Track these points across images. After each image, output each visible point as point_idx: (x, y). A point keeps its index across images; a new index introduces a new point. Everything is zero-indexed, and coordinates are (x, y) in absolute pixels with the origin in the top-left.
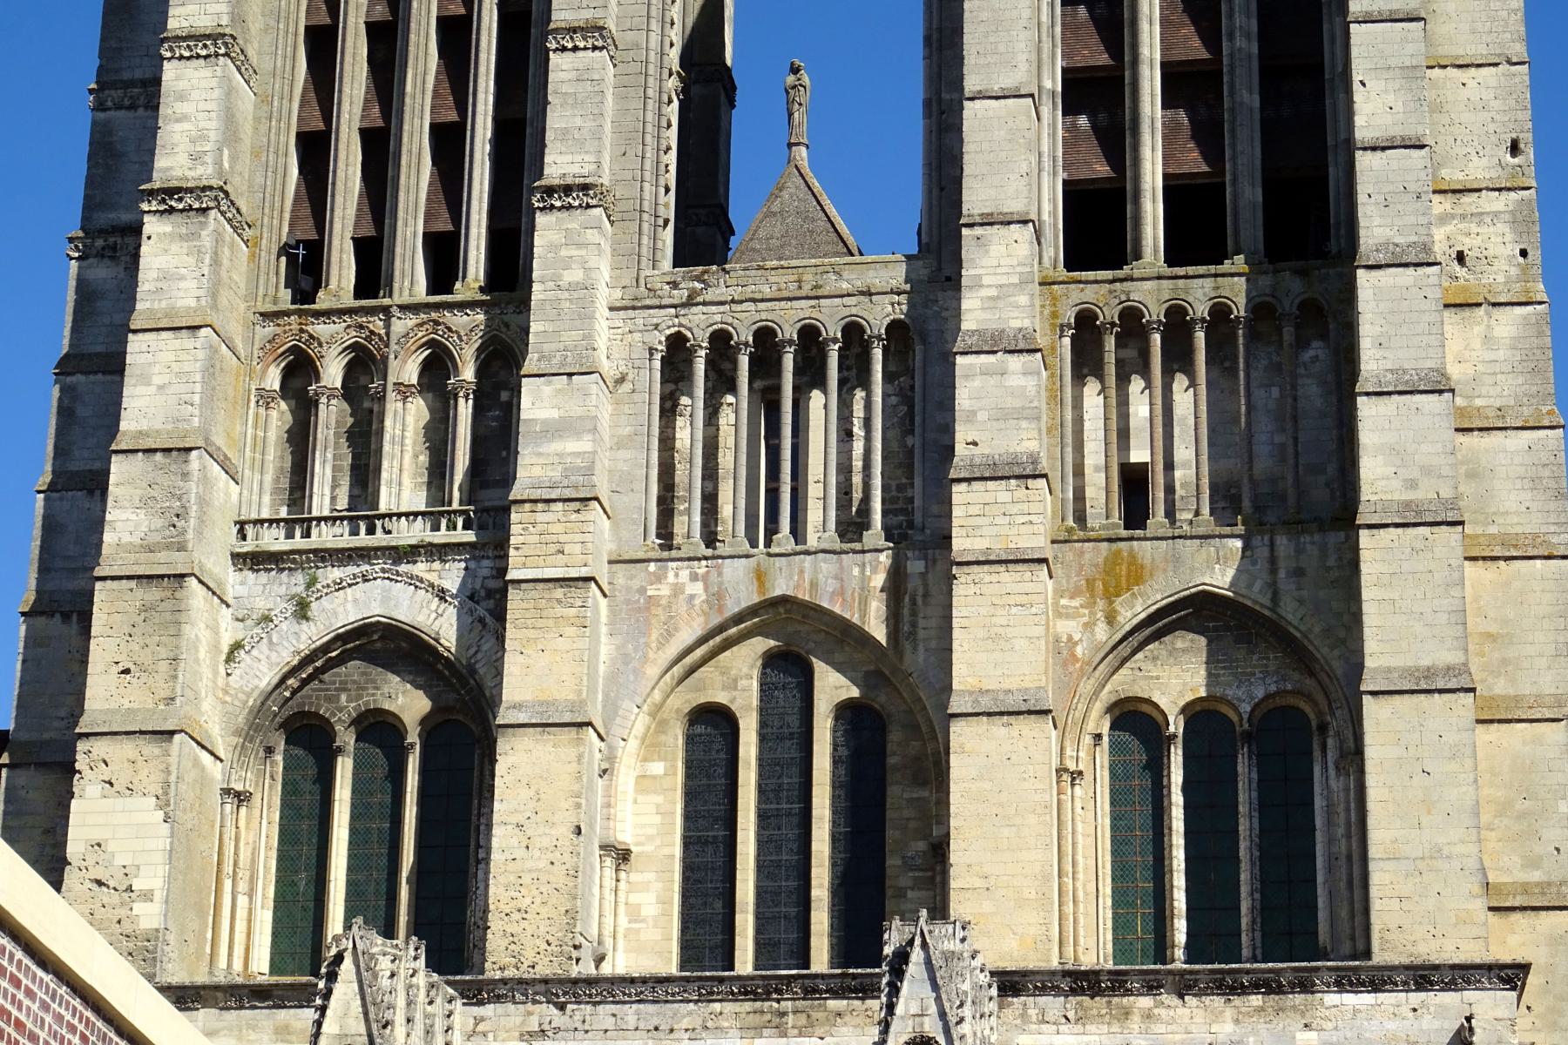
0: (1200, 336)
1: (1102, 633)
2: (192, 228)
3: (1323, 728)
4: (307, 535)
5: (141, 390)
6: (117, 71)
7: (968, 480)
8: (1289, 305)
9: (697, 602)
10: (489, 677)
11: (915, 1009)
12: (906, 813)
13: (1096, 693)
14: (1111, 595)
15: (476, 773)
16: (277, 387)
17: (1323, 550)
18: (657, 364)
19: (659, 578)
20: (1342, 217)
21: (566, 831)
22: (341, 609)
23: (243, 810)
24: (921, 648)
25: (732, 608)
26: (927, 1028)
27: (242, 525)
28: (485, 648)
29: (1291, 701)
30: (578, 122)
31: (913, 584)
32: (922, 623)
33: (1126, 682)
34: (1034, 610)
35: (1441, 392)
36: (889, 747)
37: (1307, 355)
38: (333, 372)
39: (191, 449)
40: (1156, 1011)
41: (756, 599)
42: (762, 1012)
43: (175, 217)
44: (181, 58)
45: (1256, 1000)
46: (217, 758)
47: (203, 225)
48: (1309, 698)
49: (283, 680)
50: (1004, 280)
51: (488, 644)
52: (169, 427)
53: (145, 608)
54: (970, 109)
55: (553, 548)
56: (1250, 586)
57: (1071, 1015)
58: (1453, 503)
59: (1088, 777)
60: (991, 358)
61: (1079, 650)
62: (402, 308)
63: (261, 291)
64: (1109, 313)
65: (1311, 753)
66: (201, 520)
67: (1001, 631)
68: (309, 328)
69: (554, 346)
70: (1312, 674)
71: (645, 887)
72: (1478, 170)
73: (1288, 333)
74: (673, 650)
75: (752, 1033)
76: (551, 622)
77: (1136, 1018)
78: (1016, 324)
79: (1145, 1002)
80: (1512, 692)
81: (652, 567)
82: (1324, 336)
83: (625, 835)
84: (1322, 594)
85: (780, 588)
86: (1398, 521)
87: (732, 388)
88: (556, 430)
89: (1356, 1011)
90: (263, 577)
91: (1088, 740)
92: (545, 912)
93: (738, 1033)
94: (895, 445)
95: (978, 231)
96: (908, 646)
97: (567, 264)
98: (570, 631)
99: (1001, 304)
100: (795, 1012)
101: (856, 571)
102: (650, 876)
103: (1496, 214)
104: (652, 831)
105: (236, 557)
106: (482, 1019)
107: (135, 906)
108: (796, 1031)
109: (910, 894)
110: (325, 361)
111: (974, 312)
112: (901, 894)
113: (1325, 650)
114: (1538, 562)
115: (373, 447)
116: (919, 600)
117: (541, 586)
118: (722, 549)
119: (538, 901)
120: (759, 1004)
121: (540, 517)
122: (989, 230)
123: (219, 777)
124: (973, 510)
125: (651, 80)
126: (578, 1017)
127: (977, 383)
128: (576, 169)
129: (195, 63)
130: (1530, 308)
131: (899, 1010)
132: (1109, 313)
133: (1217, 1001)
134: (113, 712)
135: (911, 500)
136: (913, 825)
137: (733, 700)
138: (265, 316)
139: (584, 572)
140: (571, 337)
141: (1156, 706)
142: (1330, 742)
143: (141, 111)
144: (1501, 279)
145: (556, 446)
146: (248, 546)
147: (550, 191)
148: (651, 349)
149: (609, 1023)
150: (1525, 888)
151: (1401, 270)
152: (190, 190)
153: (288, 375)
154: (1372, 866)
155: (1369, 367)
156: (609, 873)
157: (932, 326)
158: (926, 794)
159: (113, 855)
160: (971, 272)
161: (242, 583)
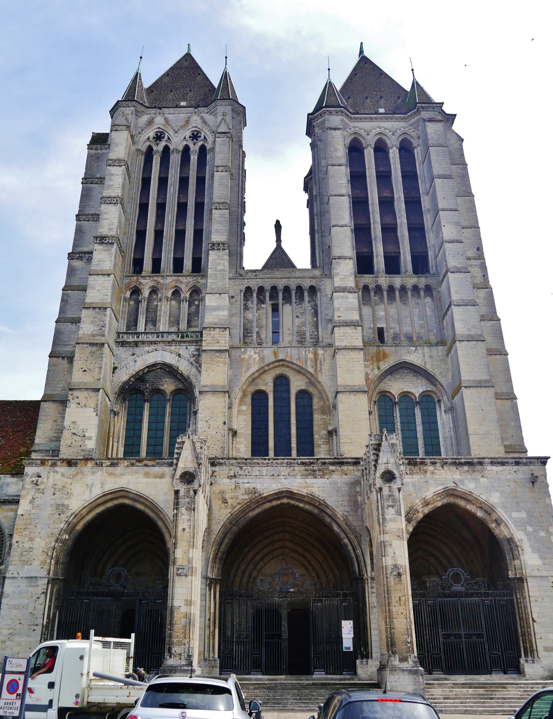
0: (397, 293)
1: (376, 372)
2: (109, 248)
3: (439, 401)
4: (138, 337)
5: (92, 291)
6: (84, 211)
8: (422, 286)
9: (256, 360)
10: (194, 379)
11: (385, 461)
12: (320, 423)
13: (375, 389)
14: (378, 360)
15: (188, 408)
16: (129, 296)
17: (438, 352)
18: (242, 294)
19: (245, 353)
20: (434, 264)
21: (221, 423)
22: (148, 359)
23: (116, 417)
24: (324, 375)
25: (267, 362)
26: (390, 467)
27: (118, 333)
28: (192, 371)
29: (429, 393)
30: (221, 228)
31: (320, 356)
32: (323, 368)
33: (383, 386)
35: (475, 306)
37: (426, 300)
38: (146, 293)
39: (107, 308)
41: (274, 360)
42: (308, 470)
43: (103, 245)
45: (466, 468)
46: (110, 400)
48: (435, 393)
49: (130, 378)
50: (345, 274)
51: (194, 370)
52: (101, 301)
53: (91, 352)
54: (333, 229)
55: (216, 341)
56: (418, 360)
57: (408, 472)
58: (481, 335)
59: (373, 413)
61: (370, 377)
62: (167, 276)
63: (125, 270)
64: (372, 286)
65: (435, 409)
66: (109, 329)
68: (140, 281)
69: (215, 286)
70: (435, 386)
71: (241, 443)
73: (422, 293)
75: (305, 477)
76: (215, 362)
77: (429, 473)
78: (350, 285)
79: (431, 468)
81: (243, 350)
82: (431, 296)
84: (439, 363)
85: (281, 357)
87: (263, 302)
88: (215, 309)
89: (497, 472)
90: (124, 349)
91: (373, 403)
92: (215, 447)
93: (300, 477)
94: (311, 320)
95: (337, 260)
96: (319, 374)
97: (219, 264)
98: (221, 365)
99: (345, 280)
100: (319, 470)
101: (304, 353)
102: (242, 439)
103: (475, 265)
104: (243, 426)
105: (116, 342)
106: (215, 471)
107: (86, 441)
108: (319, 477)
109: (322, 446)
110: (145, 290)
111: (338, 282)
112: (319, 446)
113: (441, 378)
115: (158, 314)
116: (322, 361)
117: (212, 352)
118: (263, 345)
119: (213, 444)
121: (212, 332)
122: (340, 260)
123: (110, 406)
124: (341, 335)
125: (239, 221)
126: (247, 471)
127: (340, 300)
128: (221, 240)
131: (380, 461)
132: (372, 286)
133: (453, 468)
134: (81, 382)
135: (318, 335)
136: (322, 426)
137: (267, 389)
139: (225, 348)
140: (220, 284)
141: (392, 394)
142: (442, 405)
143: (91, 222)
145: (216, 313)
146: (121, 340)
147: (213, 244)
149: (257, 473)
152: (109, 237)
153: (132, 294)
154: (470, 436)
156: (231, 438)
157: (322, 287)
158: (325, 417)
159: (79, 425)
160: (336, 271)
161: (119, 350)
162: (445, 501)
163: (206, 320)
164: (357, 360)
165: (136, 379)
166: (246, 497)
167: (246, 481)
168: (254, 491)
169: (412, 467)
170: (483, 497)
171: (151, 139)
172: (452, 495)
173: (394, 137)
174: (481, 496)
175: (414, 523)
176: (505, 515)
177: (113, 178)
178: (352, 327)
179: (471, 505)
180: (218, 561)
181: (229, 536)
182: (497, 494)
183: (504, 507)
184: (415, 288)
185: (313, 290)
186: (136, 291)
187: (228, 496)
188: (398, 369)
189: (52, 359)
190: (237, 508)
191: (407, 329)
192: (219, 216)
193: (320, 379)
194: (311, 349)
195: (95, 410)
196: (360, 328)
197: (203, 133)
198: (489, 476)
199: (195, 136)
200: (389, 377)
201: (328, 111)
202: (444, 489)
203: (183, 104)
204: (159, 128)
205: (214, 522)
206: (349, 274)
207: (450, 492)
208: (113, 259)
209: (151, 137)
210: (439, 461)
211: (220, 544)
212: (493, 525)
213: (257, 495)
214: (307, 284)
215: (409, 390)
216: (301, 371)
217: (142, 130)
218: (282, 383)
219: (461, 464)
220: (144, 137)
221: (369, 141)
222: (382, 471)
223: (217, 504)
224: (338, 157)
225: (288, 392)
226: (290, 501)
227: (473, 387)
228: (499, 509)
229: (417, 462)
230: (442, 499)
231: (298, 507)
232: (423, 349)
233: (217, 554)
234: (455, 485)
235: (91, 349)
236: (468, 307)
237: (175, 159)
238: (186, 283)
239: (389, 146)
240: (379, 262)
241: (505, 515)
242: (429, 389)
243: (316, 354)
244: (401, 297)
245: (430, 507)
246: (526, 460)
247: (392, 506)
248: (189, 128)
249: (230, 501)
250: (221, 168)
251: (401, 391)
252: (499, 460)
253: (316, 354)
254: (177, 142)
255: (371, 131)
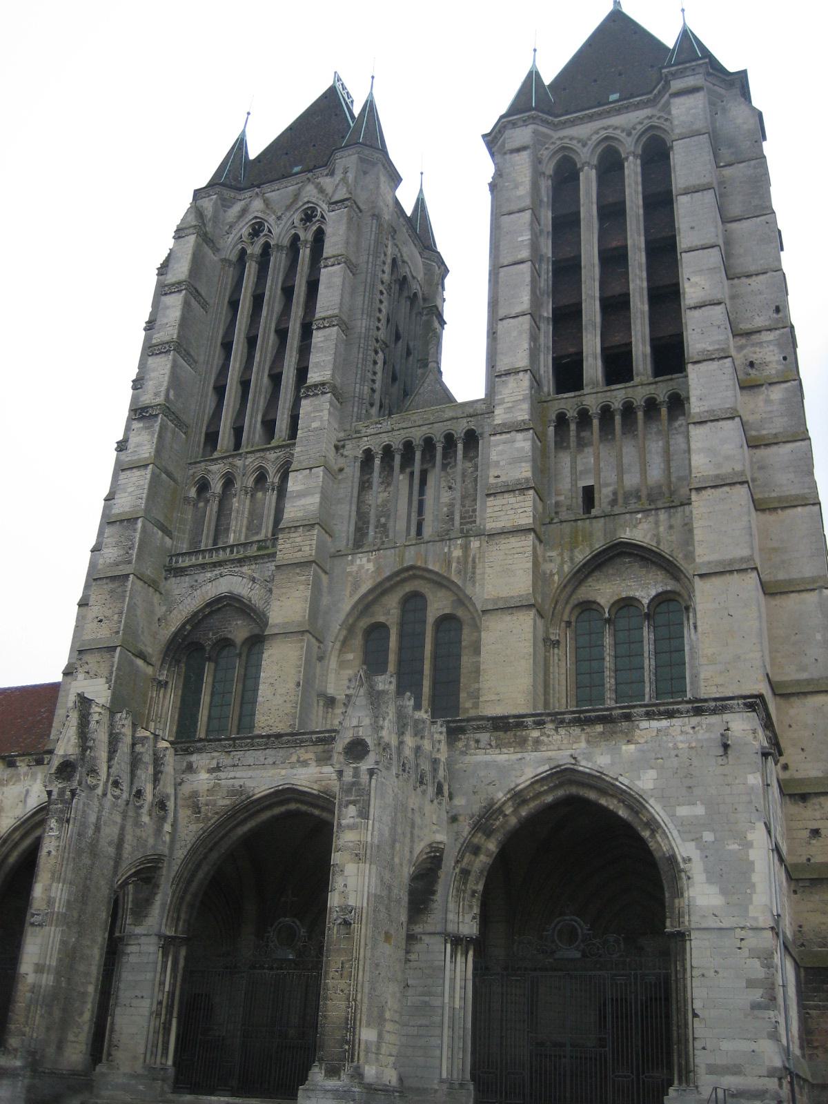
0: (618, 419)
5: (123, 495)
7: (494, 494)
11: (355, 723)
14: (573, 546)
18: (358, 464)
19: (352, 562)
21: (292, 685)
23: (162, 691)
33: (584, 593)
34: (526, 555)
35: (733, 418)
36: (464, 637)
37: (677, 424)
38: (217, 486)
39: (138, 518)
40: (542, 738)
41: (398, 567)
44: (157, 354)
45: (599, 728)
47: (156, 422)
49: (184, 625)
53: (112, 591)
57: (493, 743)
60: (508, 436)
62: (247, 453)
64: (571, 414)
65: (683, 624)
67: (509, 567)
72: (759, 322)
73: (664, 411)
74: (356, 598)
78: (520, 418)
79: (535, 734)
80: (787, 577)
81: (350, 558)
83: (331, 691)
86: (711, 484)
88: (301, 495)
89: (659, 731)
91: (563, 624)
95: (504, 378)
111: (500, 416)
114: (799, 509)
116: (477, 560)
120: (327, 746)
124: (497, 509)
126: (236, 759)
127: (500, 448)
129: (160, 356)
130: (789, 384)
132: (571, 414)
133: (576, 731)
138: (190, 464)
139: (311, 559)
141: (599, 604)
144: (773, 372)
145: (303, 501)
147: (309, 388)
148: (355, 457)
149: (251, 761)
150: (798, 682)
151: (710, 362)
152: (152, 407)
155: (695, 411)
160: (500, 397)
162: (560, 793)
163: (286, 516)
164: (519, 550)
165: (192, 627)
166: (227, 802)
167: (232, 775)
168: (240, 791)
169: (501, 734)
170: (624, 781)
171: (244, 239)
172: (571, 782)
173: (629, 139)
174: (621, 779)
175: (499, 836)
176: (662, 813)
177: (167, 312)
178: (517, 492)
179: (609, 798)
180: (184, 908)
181: (205, 867)
182: (652, 774)
183: (663, 798)
184: (651, 406)
185: (472, 439)
186: (203, 486)
187: (202, 800)
188: (611, 558)
189: (82, 608)
190: (212, 821)
191: (632, 480)
192: (323, 339)
193: (469, 591)
194: (459, 542)
195: (108, 681)
196: (531, 492)
197: (319, 210)
198: (642, 741)
199: (309, 216)
200: (596, 574)
201: (509, 122)
202: (551, 769)
203: (296, 169)
204: (256, 217)
205: (178, 846)
206: (521, 397)
207: (564, 775)
208: (155, 441)
209: (246, 233)
210: (549, 718)
211: (189, 882)
212: (646, 834)
213: (243, 797)
214: (460, 429)
215: (631, 594)
216: (441, 582)
217: (231, 227)
218: (414, 604)
219: (590, 722)
220: (231, 239)
221: (587, 156)
222: (347, 741)
223: (184, 813)
224: (519, 197)
225: (425, 622)
226: (299, 805)
227: (715, 574)
228: (652, 801)
229: (509, 723)
230: (551, 790)
231: (312, 815)
232: (657, 515)
233: (182, 898)
234: (573, 762)
235: (111, 586)
236: (721, 423)
237: (278, 261)
238: (271, 461)
239: (623, 156)
240: (593, 367)
241: (662, 813)
242: (669, 588)
243: (466, 548)
244: (624, 424)
245: (532, 805)
246: (714, 704)
247: (354, 803)
248: (298, 206)
249: (203, 809)
250: (332, 260)
251: (616, 598)
252: (662, 708)
253: (466, 548)
254: (279, 232)
255: (589, 139)
